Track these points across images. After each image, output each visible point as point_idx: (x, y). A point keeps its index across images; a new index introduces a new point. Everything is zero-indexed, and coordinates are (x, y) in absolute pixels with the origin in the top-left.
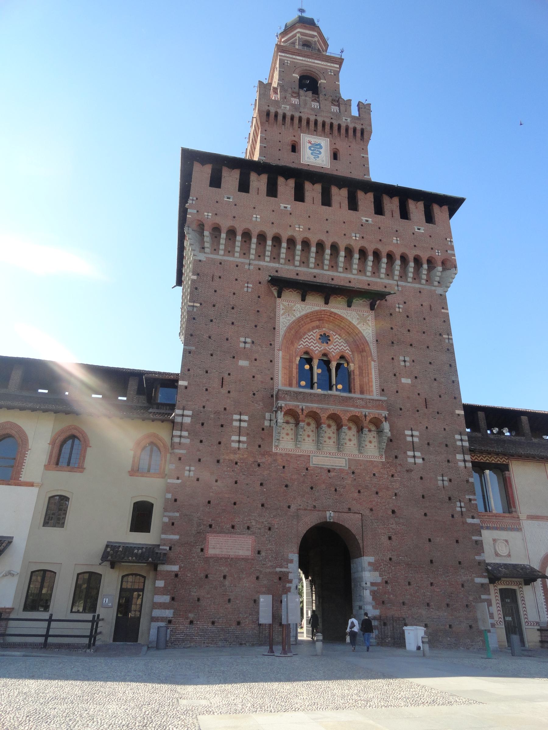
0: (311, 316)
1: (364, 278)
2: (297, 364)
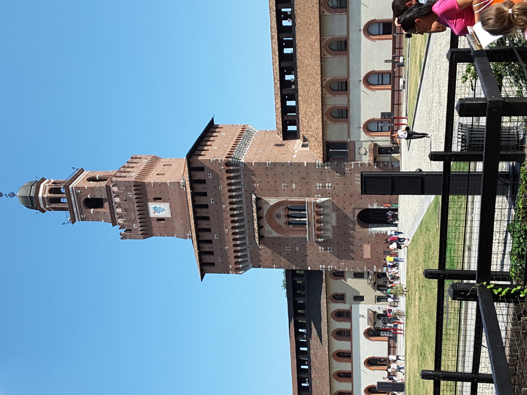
1: (244, 200)
2: (293, 227)
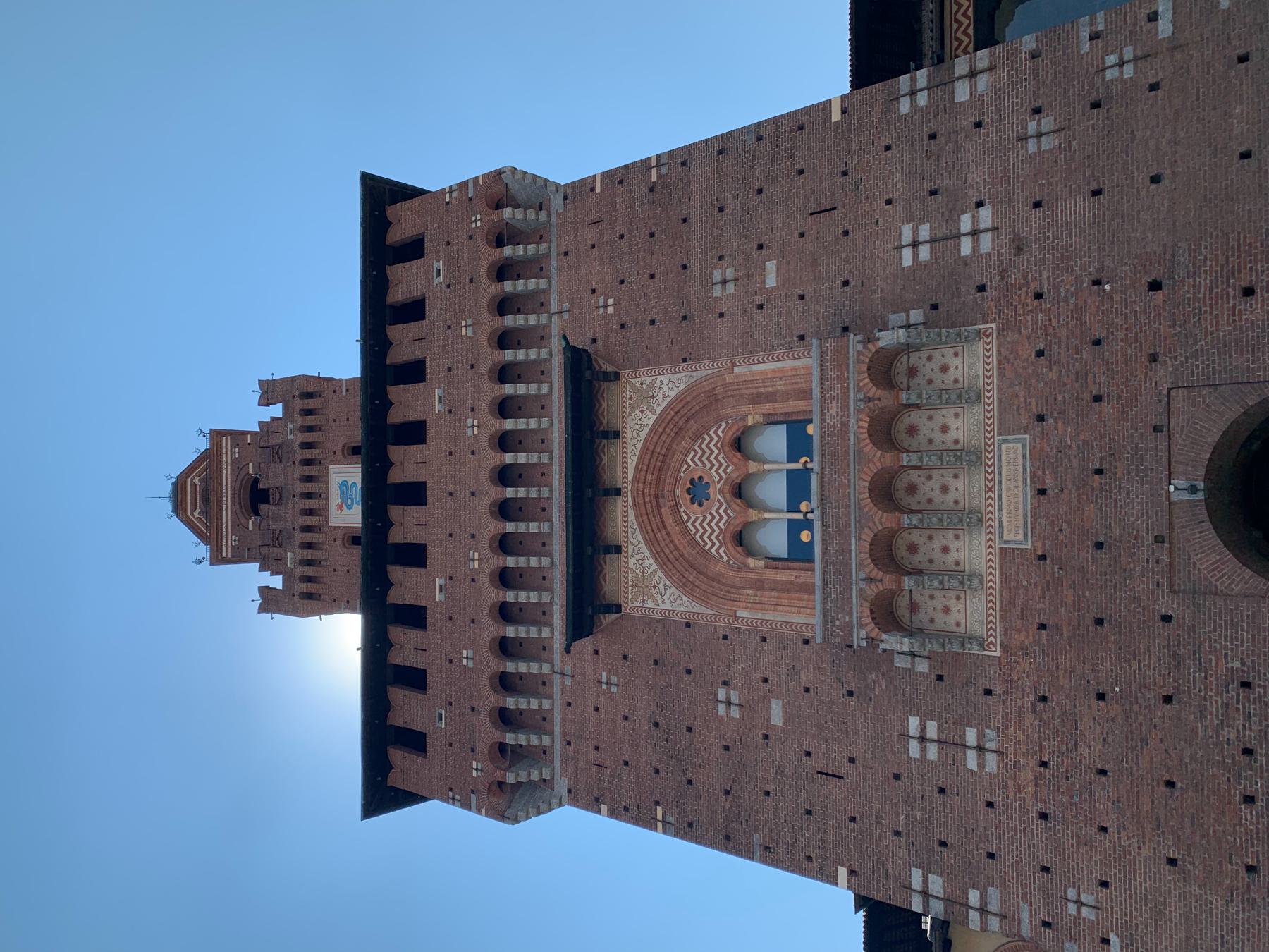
0: (650, 531)
